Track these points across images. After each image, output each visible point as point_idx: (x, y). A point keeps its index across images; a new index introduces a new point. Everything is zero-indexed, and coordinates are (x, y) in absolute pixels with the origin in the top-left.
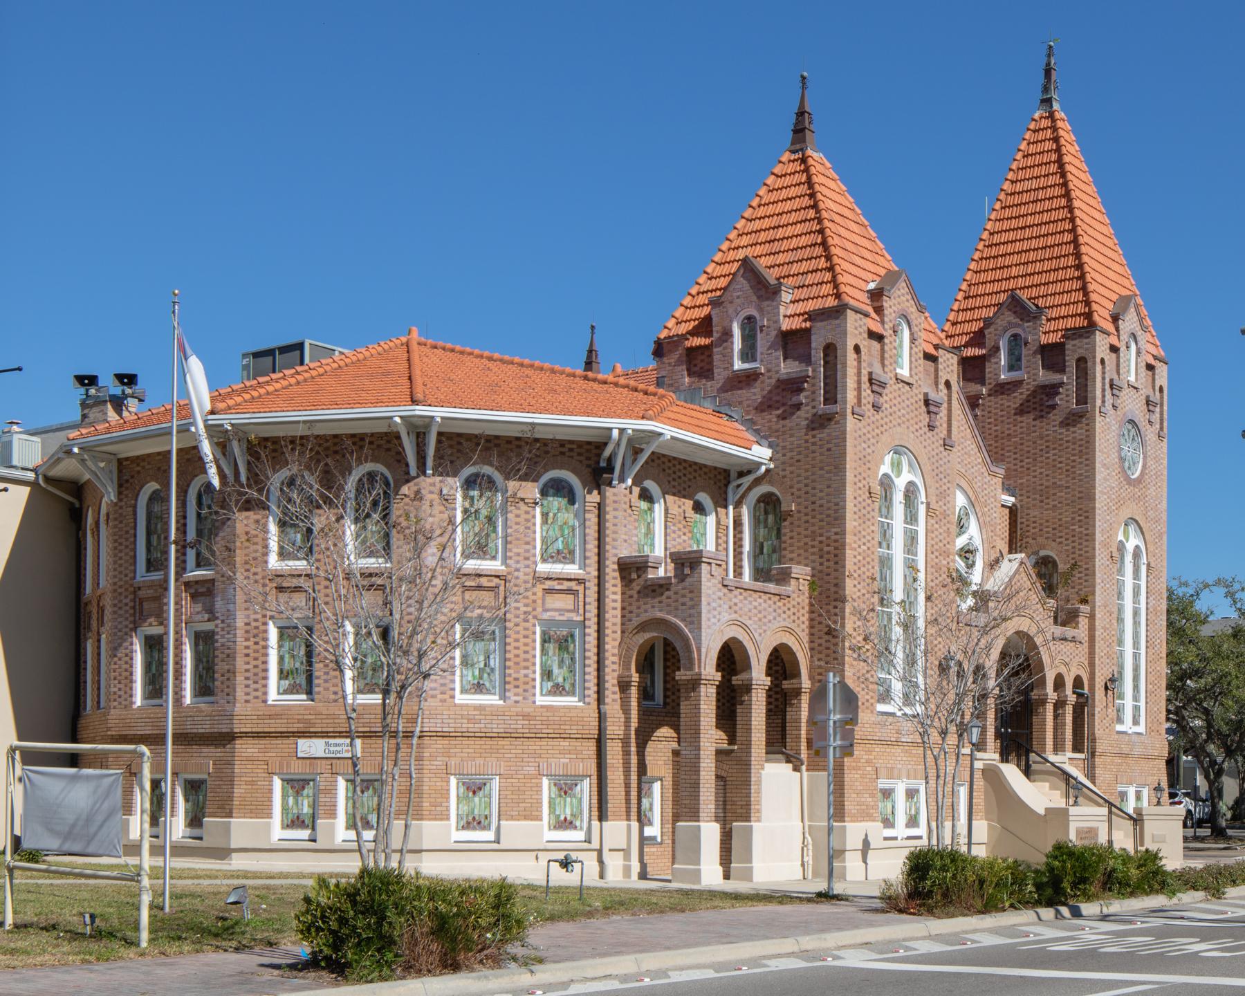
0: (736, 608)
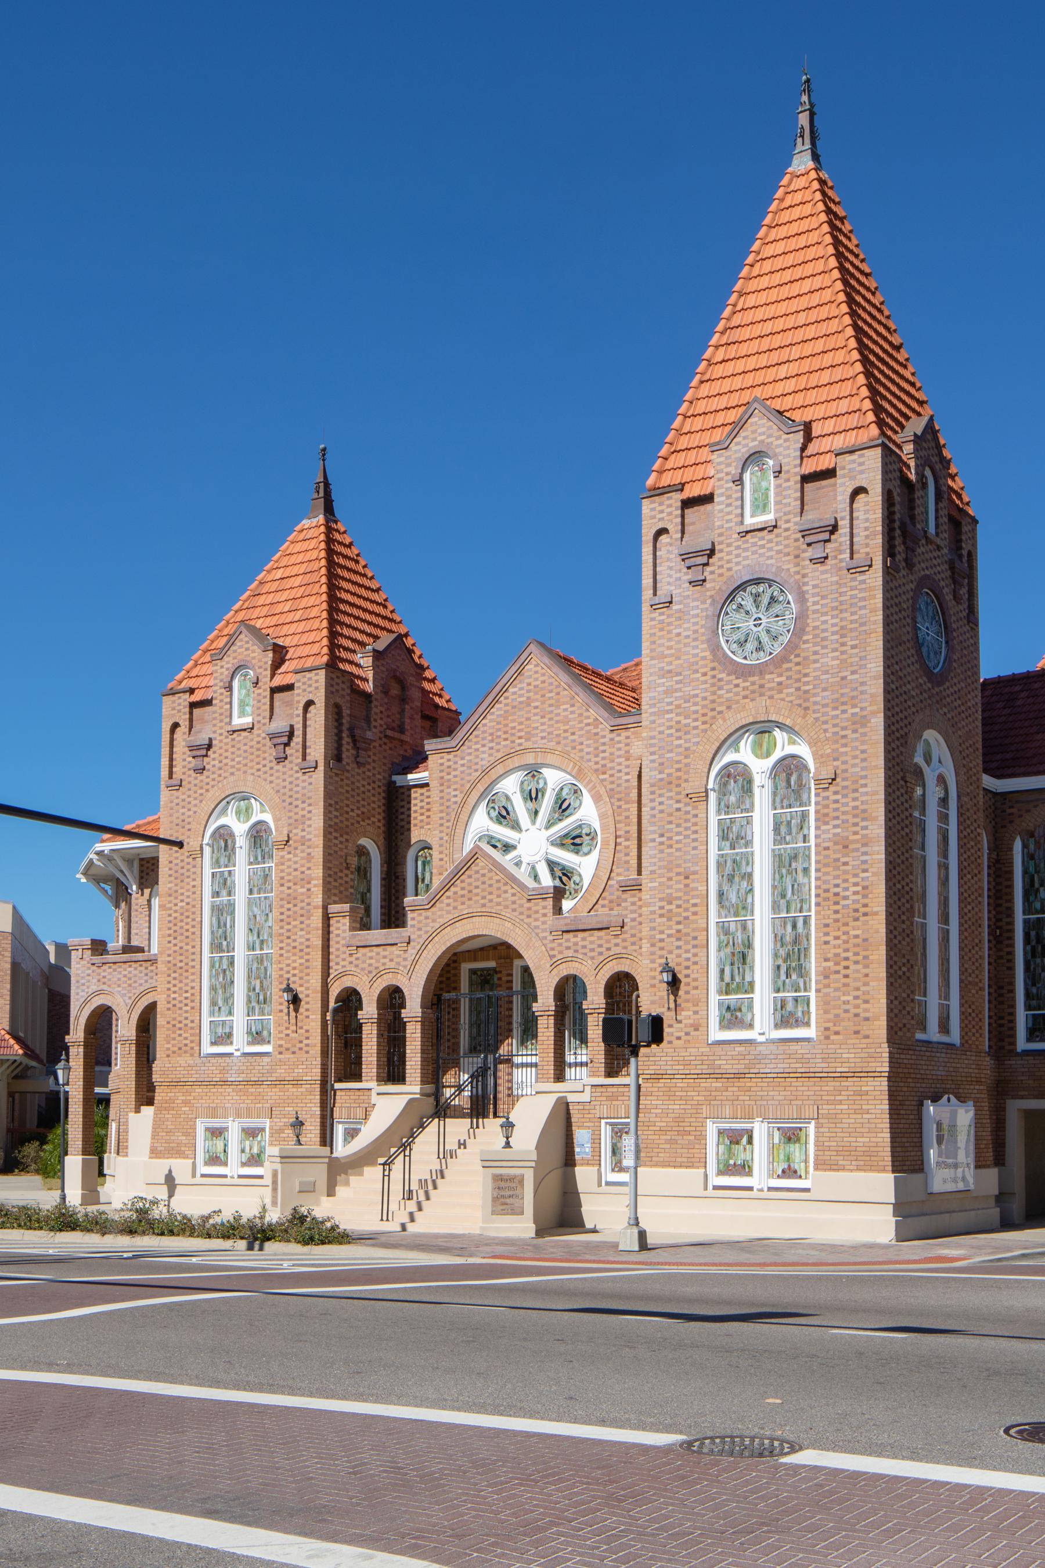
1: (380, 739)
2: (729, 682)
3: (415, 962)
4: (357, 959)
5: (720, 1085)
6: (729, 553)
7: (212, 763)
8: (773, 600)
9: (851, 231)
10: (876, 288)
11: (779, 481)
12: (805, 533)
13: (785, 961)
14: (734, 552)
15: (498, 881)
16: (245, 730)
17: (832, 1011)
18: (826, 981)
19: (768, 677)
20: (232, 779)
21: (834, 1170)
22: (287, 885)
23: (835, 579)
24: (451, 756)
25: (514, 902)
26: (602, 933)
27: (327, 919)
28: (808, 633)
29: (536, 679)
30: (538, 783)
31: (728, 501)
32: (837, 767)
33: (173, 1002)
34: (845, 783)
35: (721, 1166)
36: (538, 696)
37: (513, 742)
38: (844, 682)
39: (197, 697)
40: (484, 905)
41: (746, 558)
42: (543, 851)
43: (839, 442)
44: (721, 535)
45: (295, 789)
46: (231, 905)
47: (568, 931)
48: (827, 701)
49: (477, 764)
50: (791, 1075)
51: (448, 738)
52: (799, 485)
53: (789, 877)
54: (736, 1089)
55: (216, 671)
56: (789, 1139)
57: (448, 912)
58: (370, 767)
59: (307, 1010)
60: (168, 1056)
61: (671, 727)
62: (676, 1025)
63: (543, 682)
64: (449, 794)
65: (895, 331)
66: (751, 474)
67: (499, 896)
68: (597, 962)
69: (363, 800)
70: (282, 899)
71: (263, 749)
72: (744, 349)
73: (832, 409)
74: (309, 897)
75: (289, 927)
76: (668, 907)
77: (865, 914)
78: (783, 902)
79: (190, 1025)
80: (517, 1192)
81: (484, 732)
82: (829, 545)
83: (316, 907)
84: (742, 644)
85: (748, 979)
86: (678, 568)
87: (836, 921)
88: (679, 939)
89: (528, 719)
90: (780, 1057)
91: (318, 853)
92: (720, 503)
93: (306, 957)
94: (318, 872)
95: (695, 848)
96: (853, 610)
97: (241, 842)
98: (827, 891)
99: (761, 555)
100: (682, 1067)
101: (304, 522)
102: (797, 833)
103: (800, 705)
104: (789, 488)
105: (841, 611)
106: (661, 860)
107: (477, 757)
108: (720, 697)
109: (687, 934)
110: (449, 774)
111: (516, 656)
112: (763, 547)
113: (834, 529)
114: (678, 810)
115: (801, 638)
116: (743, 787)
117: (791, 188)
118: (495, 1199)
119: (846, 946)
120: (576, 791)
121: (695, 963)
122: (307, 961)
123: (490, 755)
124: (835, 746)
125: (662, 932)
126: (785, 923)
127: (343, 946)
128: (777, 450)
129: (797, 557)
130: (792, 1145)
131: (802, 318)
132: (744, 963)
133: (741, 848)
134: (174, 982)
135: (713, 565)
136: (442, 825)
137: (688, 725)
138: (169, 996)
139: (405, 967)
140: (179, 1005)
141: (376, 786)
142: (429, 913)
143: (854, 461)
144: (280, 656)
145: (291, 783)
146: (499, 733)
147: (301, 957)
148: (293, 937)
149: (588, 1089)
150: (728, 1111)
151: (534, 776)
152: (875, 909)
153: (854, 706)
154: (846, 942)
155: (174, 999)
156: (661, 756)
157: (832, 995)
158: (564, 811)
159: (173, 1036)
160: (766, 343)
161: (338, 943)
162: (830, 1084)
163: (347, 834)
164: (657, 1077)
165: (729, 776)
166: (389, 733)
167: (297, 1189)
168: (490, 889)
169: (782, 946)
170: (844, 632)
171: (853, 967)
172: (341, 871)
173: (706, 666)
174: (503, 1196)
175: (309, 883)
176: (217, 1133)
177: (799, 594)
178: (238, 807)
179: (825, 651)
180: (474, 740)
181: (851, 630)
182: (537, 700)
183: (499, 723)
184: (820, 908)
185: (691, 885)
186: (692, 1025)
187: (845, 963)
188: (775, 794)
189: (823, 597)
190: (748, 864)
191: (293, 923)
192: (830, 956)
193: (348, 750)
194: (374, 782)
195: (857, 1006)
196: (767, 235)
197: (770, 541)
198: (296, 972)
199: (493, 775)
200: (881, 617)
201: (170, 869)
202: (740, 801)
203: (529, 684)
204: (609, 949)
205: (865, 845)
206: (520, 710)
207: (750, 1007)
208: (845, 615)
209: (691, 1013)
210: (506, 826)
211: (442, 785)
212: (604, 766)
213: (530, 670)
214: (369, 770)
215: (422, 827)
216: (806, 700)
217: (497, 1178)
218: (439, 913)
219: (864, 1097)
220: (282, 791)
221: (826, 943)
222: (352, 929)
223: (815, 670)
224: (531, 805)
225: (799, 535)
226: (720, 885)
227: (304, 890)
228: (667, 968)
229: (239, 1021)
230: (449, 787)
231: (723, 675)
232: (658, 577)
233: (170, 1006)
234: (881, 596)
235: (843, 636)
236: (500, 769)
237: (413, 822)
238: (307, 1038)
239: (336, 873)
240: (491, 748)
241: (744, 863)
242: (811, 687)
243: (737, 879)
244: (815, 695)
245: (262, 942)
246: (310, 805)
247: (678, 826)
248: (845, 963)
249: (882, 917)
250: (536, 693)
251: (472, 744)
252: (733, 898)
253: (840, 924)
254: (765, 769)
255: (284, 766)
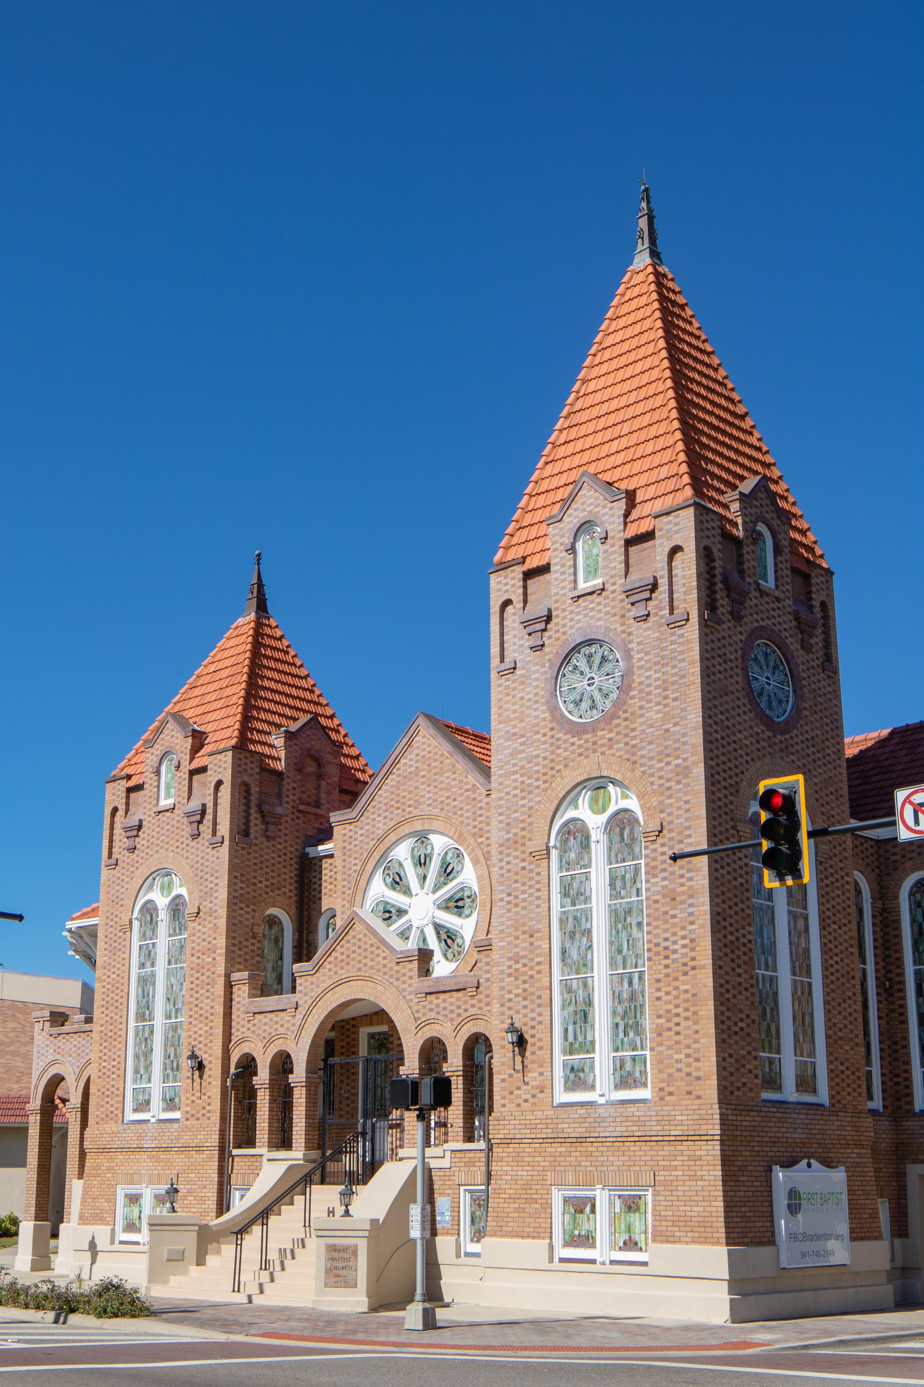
0: (60, 1050)
1: (293, 813)
2: (566, 741)
3: (301, 1027)
4: (254, 1025)
5: (564, 1149)
6: (564, 618)
7: (142, 842)
8: (604, 659)
9: (692, 316)
10: (719, 365)
11: (605, 547)
12: (628, 593)
13: (623, 1019)
14: (569, 617)
15: (372, 945)
16: (167, 810)
17: (666, 1071)
18: (659, 1039)
19: (599, 733)
20: (156, 856)
21: (671, 1242)
22: (197, 955)
23: (657, 635)
24: (352, 827)
25: (385, 966)
26: (460, 994)
27: (229, 987)
28: (633, 689)
29: (423, 750)
30: (426, 849)
31: (563, 570)
32: (664, 819)
33: (103, 1071)
34: (671, 835)
35: (567, 1237)
36: (425, 766)
37: (404, 810)
38: (668, 734)
39: (132, 783)
40: (359, 970)
41: (579, 621)
42: (430, 915)
43: (658, 506)
44: (556, 601)
45: (206, 864)
46: (153, 975)
47: (431, 993)
48: (652, 754)
49: (373, 833)
50: (629, 1139)
51: (350, 810)
52: (623, 549)
53: (624, 933)
54: (578, 1154)
55: (147, 758)
56: (630, 1208)
57: (330, 977)
58: (281, 841)
59: (210, 1076)
60: (97, 1123)
61: (516, 788)
62: (524, 1087)
63: (430, 752)
64: (350, 862)
65: (740, 402)
66: (584, 542)
67: (372, 960)
68: (455, 1024)
69: (273, 871)
70: (192, 969)
71: (182, 827)
72: (583, 430)
73: (654, 476)
74: (214, 966)
75: (198, 995)
76: (515, 966)
77: (694, 968)
78: (619, 957)
79: (116, 1092)
80: (351, 1264)
81: (380, 802)
82: (650, 603)
83: (219, 976)
84: (577, 703)
85: (589, 1038)
86: (521, 635)
87: (667, 975)
88: (525, 999)
89: (417, 788)
90: (618, 1119)
91: (222, 923)
92: (556, 572)
93: (211, 1024)
94: (222, 942)
95: (538, 906)
96: (673, 663)
97: (163, 916)
98: (657, 945)
99: (592, 618)
100: (528, 1131)
101: (239, 620)
102: (631, 887)
103: (628, 760)
104: (614, 552)
105: (663, 666)
106: (509, 919)
107: (374, 826)
108: (559, 755)
109: (532, 994)
110: (350, 844)
111: (405, 730)
112: (593, 609)
113: (654, 587)
114: (523, 868)
115: (628, 694)
116: (581, 843)
117: (632, 283)
118: (328, 1271)
119: (677, 1002)
120: (459, 855)
121: (540, 1023)
122: (211, 1028)
123: (385, 824)
124: (662, 798)
125: (510, 992)
126: (622, 979)
127: (243, 1013)
128: (604, 519)
129: (623, 616)
130: (632, 1215)
131: (633, 397)
132: (586, 1022)
133: (581, 904)
134: (104, 1051)
135: (551, 630)
136: (344, 893)
137: (530, 785)
138: (100, 1064)
139: (293, 1032)
140: (108, 1073)
141: (287, 858)
142: (313, 979)
143: (670, 522)
144: (198, 740)
145: (202, 858)
146: (392, 803)
147: (206, 1025)
148: (200, 1005)
149: (448, 1154)
150: (570, 1178)
151: (422, 842)
152: (703, 962)
153: (677, 758)
154: (676, 997)
155: (104, 1067)
156: (508, 817)
157: (665, 1053)
158: (449, 874)
159: (102, 1103)
160: (602, 423)
161: (238, 1010)
162: (666, 1148)
163: (254, 904)
164: (507, 1141)
165: (569, 833)
166: (302, 807)
167: (166, 1258)
168: (365, 954)
169: (620, 1003)
170: (666, 685)
171: (684, 1023)
172: (247, 940)
173: (545, 727)
174: (336, 1268)
175: (214, 952)
176: (134, 1199)
177: (625, 651)
178: (162, 883)
179: (650, 705)
180: (372, 810)
181: (672, 683)
182: (424, 770)
183: (392, 793)
184: (652, 963)
185: (536, 944)
186: (538, 1087)
187: (676, 1020)
188: (610, 849)
189: (647, 653)
190: (587, 920)
191: (201, 991)
192: (662, 1012)
193: (256, 825)
194: (285, 854)
195: (688, 1065)
196: (608, 327)
197: (599, 604)
198: (202, 1039)
199: (387, 842)
200: (699, 669)
201: (106, 943)
202: (580, 857)
203: (417, 755)
204: (466, 1010)
205: (691, 897)
206: (410, 779)
207: (592, 1068)
208: (666, 669)
209: (536, 1074)
210: (399, 891)
211: (344, 854)
212: (481, 829)
213: (418, 741)
214: (280, 843)
215: (331, 896)
216: (634, 754)
217: (331, 1248)
218: (322, 978)
219: (698, 1163)
220: (196, 866)
221: (659, 999)
222: (251, 996)
223: (641, 724)
224: (420, 870)
225: (624, 596)
226: (563, 943)
227: (210, 959)
228: (512, 1029)
229: (156, 1088)
230: (350, 856)
231: (561, 735)
232: (505, 645)
233: (101, 1074)
234: (698, 648)
235: (665, 689)
236: (393, 837)
237: (323, 891)
238: (209, 1104)
239: (240, 942)
240: (386, 817)
241: (584, 920)
242: (638, 741)
243: (578, 936)
244: (642, 749)
245: (177, 1010)
246: (217, 878)
247: (523, 884)
248: (676, 1020)
249: (709, 970)
250: (423, 763)
251: (369, 815)
252: (574, 954)
253: (670, 979)
254: (600, 824)
255: (198, 843)
